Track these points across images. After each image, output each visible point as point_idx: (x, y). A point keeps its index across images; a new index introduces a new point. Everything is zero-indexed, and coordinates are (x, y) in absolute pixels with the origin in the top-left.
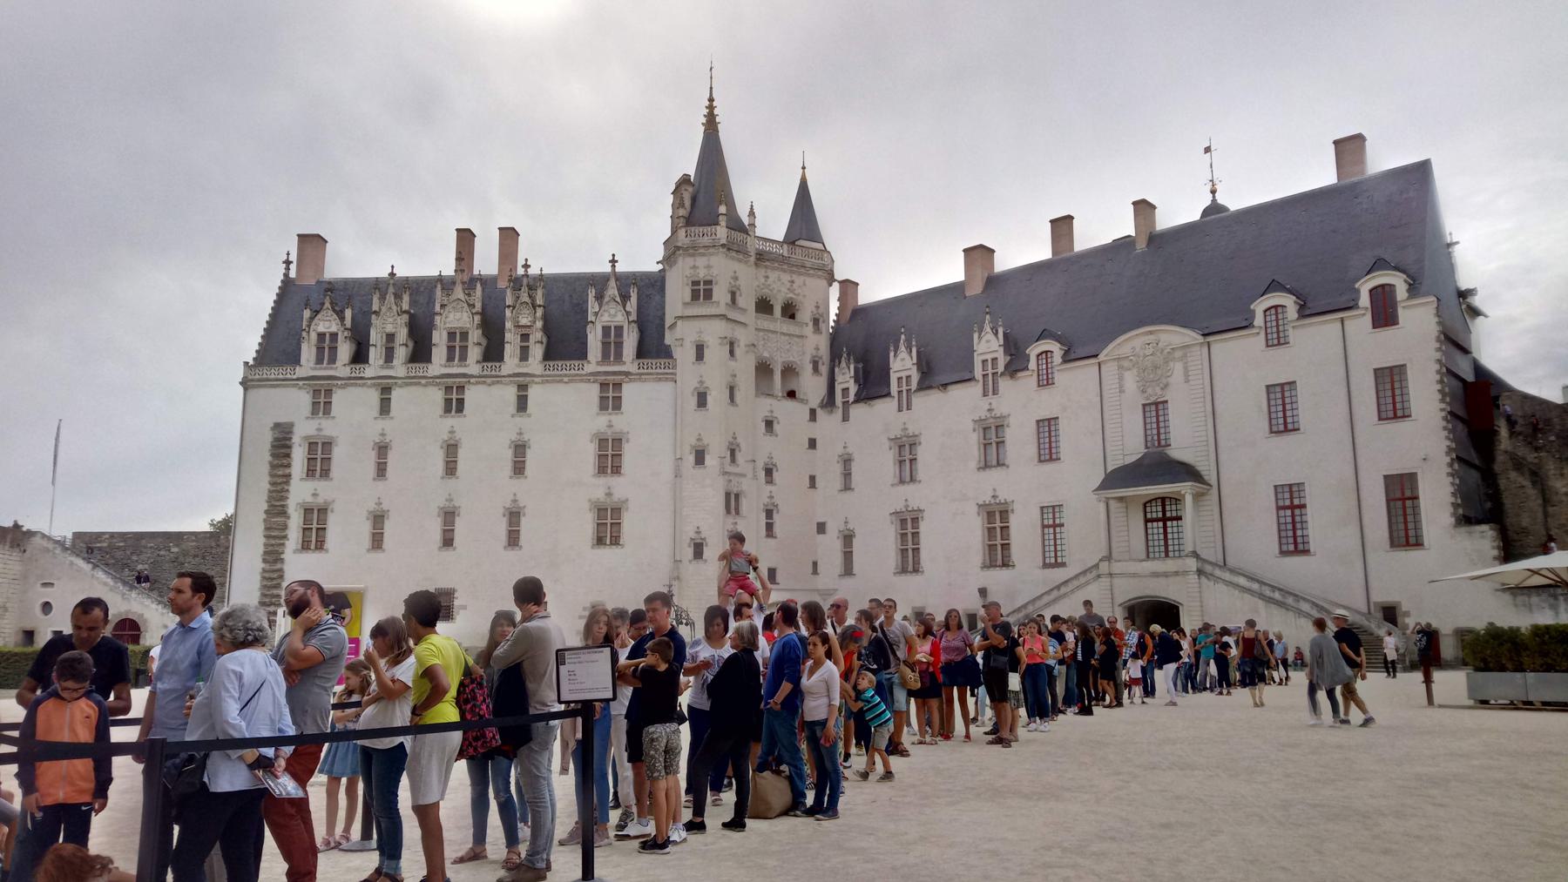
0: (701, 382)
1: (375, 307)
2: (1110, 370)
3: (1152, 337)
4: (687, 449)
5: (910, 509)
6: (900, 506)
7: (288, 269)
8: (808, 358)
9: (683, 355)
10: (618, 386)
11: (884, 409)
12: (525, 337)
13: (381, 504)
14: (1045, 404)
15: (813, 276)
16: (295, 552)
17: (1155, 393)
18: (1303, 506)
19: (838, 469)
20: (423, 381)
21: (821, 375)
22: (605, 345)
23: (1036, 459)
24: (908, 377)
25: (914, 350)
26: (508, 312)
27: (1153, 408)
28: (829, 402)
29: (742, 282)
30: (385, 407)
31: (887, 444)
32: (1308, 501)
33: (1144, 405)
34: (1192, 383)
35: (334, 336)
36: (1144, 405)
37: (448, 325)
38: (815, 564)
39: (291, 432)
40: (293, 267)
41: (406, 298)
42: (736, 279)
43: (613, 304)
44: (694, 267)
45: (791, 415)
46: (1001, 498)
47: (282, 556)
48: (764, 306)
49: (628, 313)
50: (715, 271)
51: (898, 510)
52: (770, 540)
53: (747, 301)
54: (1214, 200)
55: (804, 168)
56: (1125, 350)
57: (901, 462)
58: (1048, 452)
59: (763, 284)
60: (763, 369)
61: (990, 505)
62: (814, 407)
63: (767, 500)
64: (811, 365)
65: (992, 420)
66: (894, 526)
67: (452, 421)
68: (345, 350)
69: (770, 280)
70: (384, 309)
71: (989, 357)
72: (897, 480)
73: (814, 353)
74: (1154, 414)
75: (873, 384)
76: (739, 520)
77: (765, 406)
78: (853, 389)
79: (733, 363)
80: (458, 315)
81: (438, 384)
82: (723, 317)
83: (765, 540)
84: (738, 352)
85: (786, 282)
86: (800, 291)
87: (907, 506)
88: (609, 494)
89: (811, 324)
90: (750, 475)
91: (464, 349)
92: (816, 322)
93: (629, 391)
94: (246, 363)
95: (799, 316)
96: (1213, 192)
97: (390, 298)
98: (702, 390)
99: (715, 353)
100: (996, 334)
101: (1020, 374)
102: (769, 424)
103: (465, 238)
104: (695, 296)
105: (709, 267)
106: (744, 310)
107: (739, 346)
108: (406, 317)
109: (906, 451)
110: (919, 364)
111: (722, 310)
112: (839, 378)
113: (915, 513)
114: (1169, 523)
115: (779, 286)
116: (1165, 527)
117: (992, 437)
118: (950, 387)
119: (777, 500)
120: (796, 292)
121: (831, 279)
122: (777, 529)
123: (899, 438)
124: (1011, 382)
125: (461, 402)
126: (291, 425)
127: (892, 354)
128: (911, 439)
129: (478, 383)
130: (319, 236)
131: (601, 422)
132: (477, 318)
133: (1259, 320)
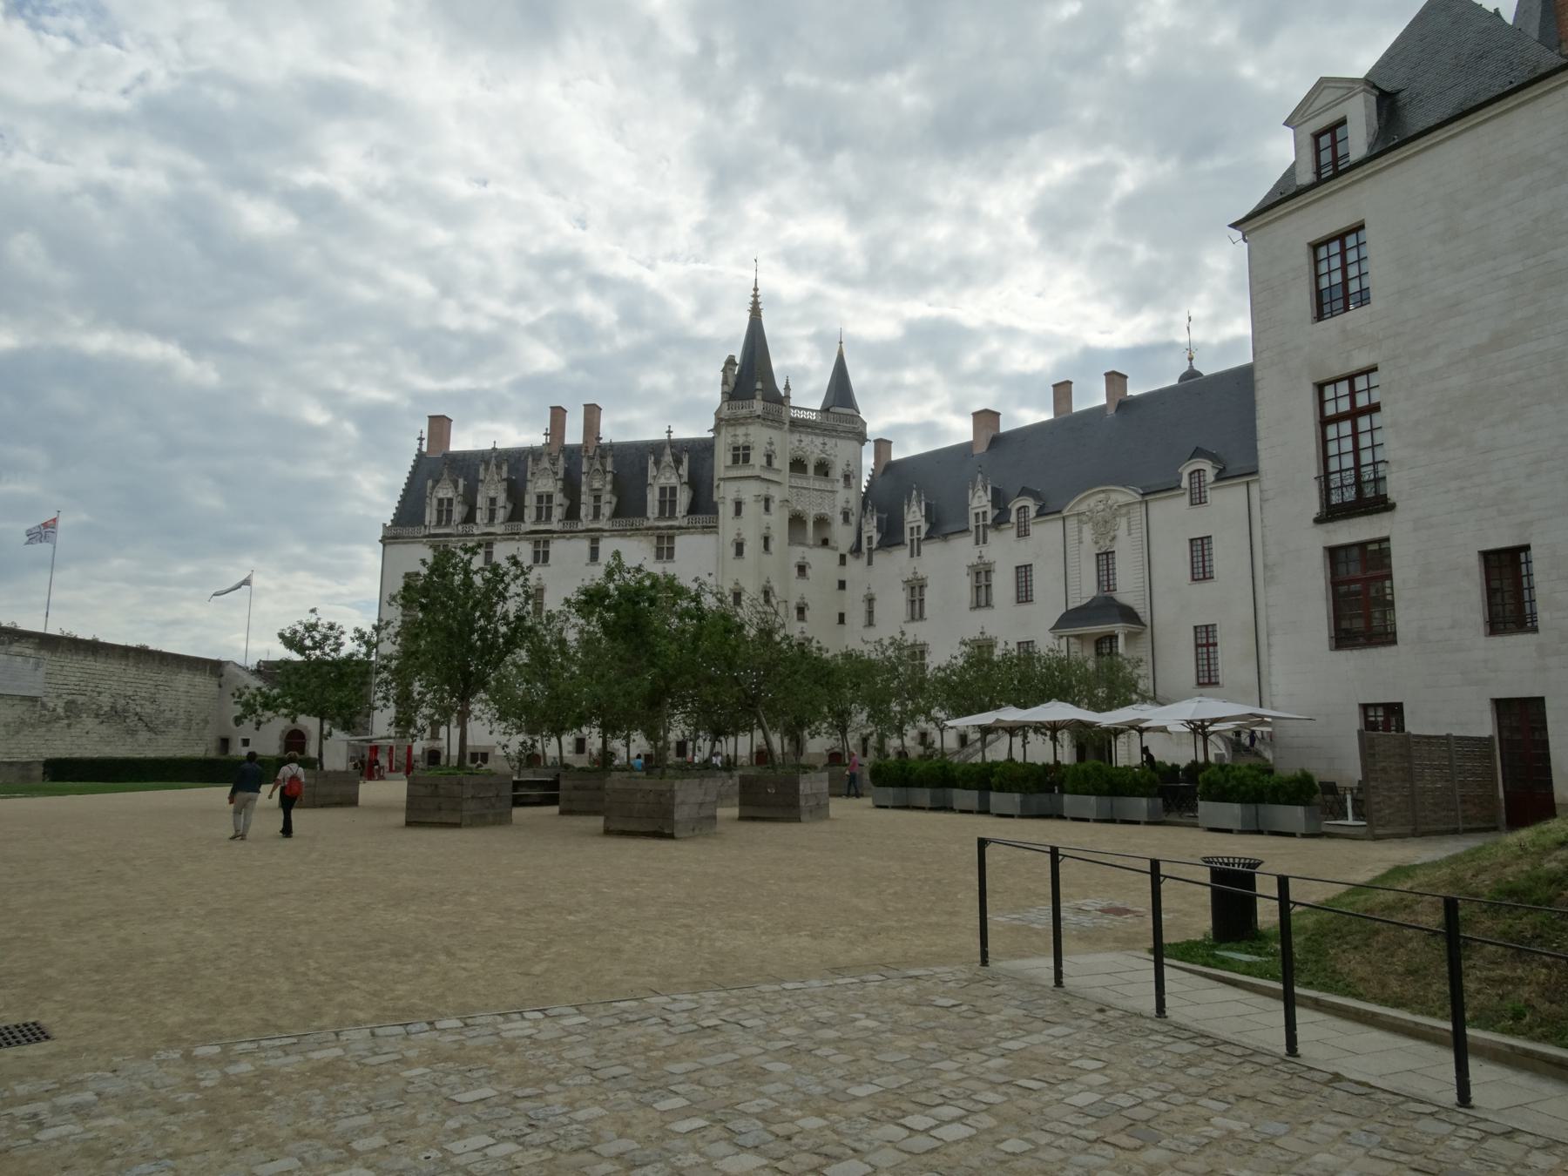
0: (739, 535)
1: (481, 477)
2: (1072, 524)
3: (1102, 496)
7: (421, 444)
8: (839, 510)
9: (726, 511)
10: (671, 538)
11: (901, 555)
12: (597, 498)
14: (1198, 522)
15: (844, 438)
17: (1105, 545)
18: (1215, 645)
19: (863, 607)
20: (517, 537)
22: (662, 503)
23: (1014, 601)
24: (919, 527)
25: (923, 504)
26: (584, 478)
27: (1105, 556)
28: (856, 550)
29: (777, 448)
31: (902, 585)
32: (1218, 640)
33: (1098, 555)
34: (1134, 536)
35: (450, 501)
36: (1098, 555)
37: (537, 490)
40: (425, 443)
41: (505, 468)
42: (771, 444)
43: (668, 469)
44: (735, 435)
45: (822, 562)
46: (988, 635)
48: (798, 465)
49: (680, 476)
50: (751, 439)
53: (783, 462)
54: (1191, 366)
55: (841, 343)
56: (1083, 507)
57: (913, 602)
58: (1024, 595)
60: (797, 521)
61: (979, 640)
62: (843, 552)
64: (841, 517)
65: (981, 566)
68: (458, 511)
69: (803, 444)
70: (488, 478)
71: (980, 510)
72: (909, 617)
74: (1105, 562)
75: (891, 536)
77: (798, 553)
78: (876, 538)
79: (766, 518)
80: (545, 481)
81: (528, 539)
82: (758, 478)
84: (773, 507)
85: (819, 445)
89: (842, 480)
91: (549, 509)
92: (847, 478)
93: (681, 542)
94: (384, 525)
95: (831, 473)
96: (1191, 359)
97: (493, 468)
98: (739, 541)
99: (752, 509)
100: (986, 491)
101: (1003, 526)
102: (802, 569)
103: (558, 414)
104: (735, 459)
105: (746, 435)
106: (779, 471)
108: (505, 484)
109: (916, 589)
110: (928, 517)
111: (757, 472)
112: (865, 528)
115: (813, 448)
117: (982, 576)
118: (951, 537)
121: (861, 438)
124: (996, 533)
125: (546, 554)
127: (906, 507)
129: (559, 538)
130: (444, 416)
132: (560, 484)
133: (1185, 483)
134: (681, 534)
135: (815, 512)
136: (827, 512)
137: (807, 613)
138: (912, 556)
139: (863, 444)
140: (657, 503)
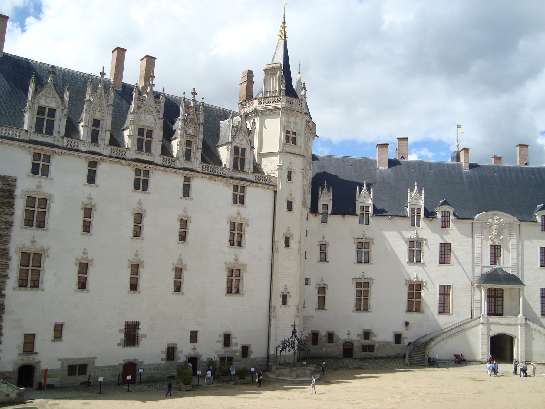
5: (365, 277)
6: (359, 275)
11: (352, 221)
13: (87, 254)
16: (14, 289)
30: (91, 178)
37: (140, 123)
39: (14, 186)
47: (3, 292)
51: (358, 277)
67: (140, 195)
88: (236, 260)
91: (149, 143)
113: (368, 280)
114: (496, 299)
116: (495, 300)
125: (146, 182)
126: (15, 180)
128: (368, 240)
129: (162, 170)
131: (234, 210)
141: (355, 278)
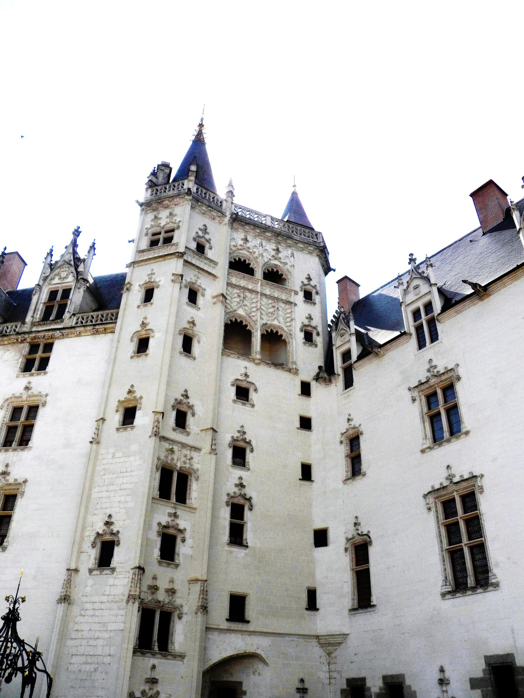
0: (144, 324)
4: (113, 404)
5: (456, 480)
8: (299, 325)
21: (316, 346)
31: (408, 395)
38: (312, 594)
51: (437, 486)
52: (236, 550)
59: (241, 245)
63: (233, 490)
66: (432, 514)
69: (249, 245)
73: (306, 322)
76: (181, 511)
78: (355, 353)
79: (190, 311)
83: (227, 548)
84: (200, 300)
86: (287, 261)
87: (450, 478)
89: (301, 294)
90: (206, 447)
106: (214, 263)
107: (203, 295)
112: (337, 341)
119: (249, 492)
120: (282, 261)
122: (249, 535)
123: (427, 382)
128: (443, 378)
134: (63, 336)
135: (264, 322)
136: (282, 325)
137: (250, 457)
138: (421, 344)
139: (326, 274)
140: (41, 307)
141: (430, 490)
